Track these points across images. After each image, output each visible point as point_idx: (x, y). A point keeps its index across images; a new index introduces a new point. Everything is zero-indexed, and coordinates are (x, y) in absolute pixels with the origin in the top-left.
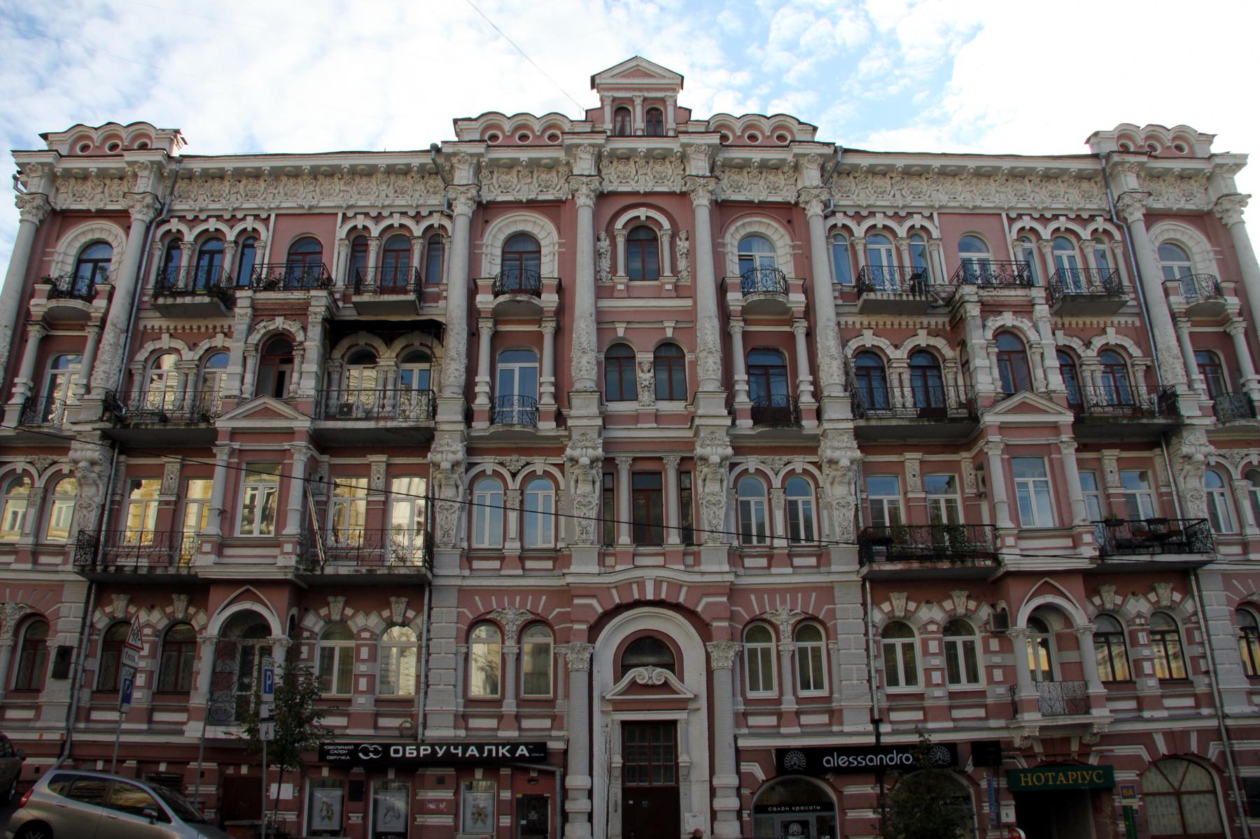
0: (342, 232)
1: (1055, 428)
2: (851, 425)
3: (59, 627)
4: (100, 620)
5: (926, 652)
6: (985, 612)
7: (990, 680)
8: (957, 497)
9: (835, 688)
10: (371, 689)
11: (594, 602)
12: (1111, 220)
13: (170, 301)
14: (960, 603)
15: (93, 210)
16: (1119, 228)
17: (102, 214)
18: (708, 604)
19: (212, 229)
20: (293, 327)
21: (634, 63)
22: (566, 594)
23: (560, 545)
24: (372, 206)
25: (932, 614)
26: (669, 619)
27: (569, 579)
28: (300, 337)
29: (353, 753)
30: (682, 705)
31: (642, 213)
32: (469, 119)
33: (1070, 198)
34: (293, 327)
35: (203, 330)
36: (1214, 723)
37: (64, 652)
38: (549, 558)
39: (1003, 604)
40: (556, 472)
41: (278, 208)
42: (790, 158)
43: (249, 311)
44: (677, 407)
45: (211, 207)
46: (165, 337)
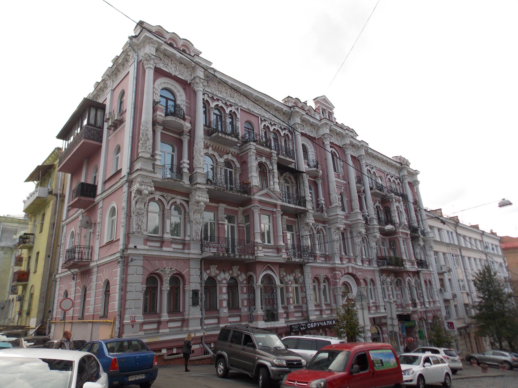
0: (262, 126)
1: (407, 234)
2: (378, 227)
3: (191, 281)
4: (205, 277)
5: (388, 290)
6: (396, 280)
7: (397, 298)
8: (385, 248)
9: (377, 299)
10: (294, 303)
11: (339, 272)
12: (400, 180)
13: (224, 136)
14: (392, 277)
15: (173, 74)
16: (401, 182)
17: (175, 79)
18: (359, 275)
19: (220, 105)
20: (268, 163)
21: (324, 97)
22: (333, 269)
23: (327, 253)
24: (269, 119)
25: (389, 280)
26: (349, 278)
27: (337, 266)
28: (271, 167)
29: (299, 328)
31: (333, 150)
32: (292, 98)
33: (393, 172)
34: (268, 163)
35: (222, 150)
36: (425, 309)
37: (195, 293)
38: (324, 257)
39: (400, 278)
40: (322, 228)
41: (241, 106)
42: (360, 145)
43: (255, 151)
44: (343, 213)
45: (219, 95)
46: (210, 148)
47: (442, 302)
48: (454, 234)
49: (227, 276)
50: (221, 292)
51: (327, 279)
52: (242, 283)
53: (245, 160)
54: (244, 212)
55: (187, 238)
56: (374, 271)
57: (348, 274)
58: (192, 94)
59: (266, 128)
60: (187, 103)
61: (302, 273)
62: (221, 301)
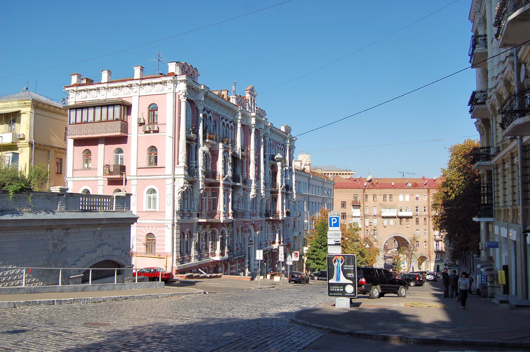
0: (221, 123)
25: (269, 226)
30: (251, 244)
47: (292, 238)
48: (307, 185)
49: (204, 231)
50: (202, 241)
51: (242, 228)
52: (209, 234)
53: (216, 154)
54: (212, 190)
55: (192, 210)
56: (262, 220)
57: (252, 224)
58: (196, 111)
59: (223, 123)
60: (192, 117)
61: (232, 226)
62: (202, 246)
